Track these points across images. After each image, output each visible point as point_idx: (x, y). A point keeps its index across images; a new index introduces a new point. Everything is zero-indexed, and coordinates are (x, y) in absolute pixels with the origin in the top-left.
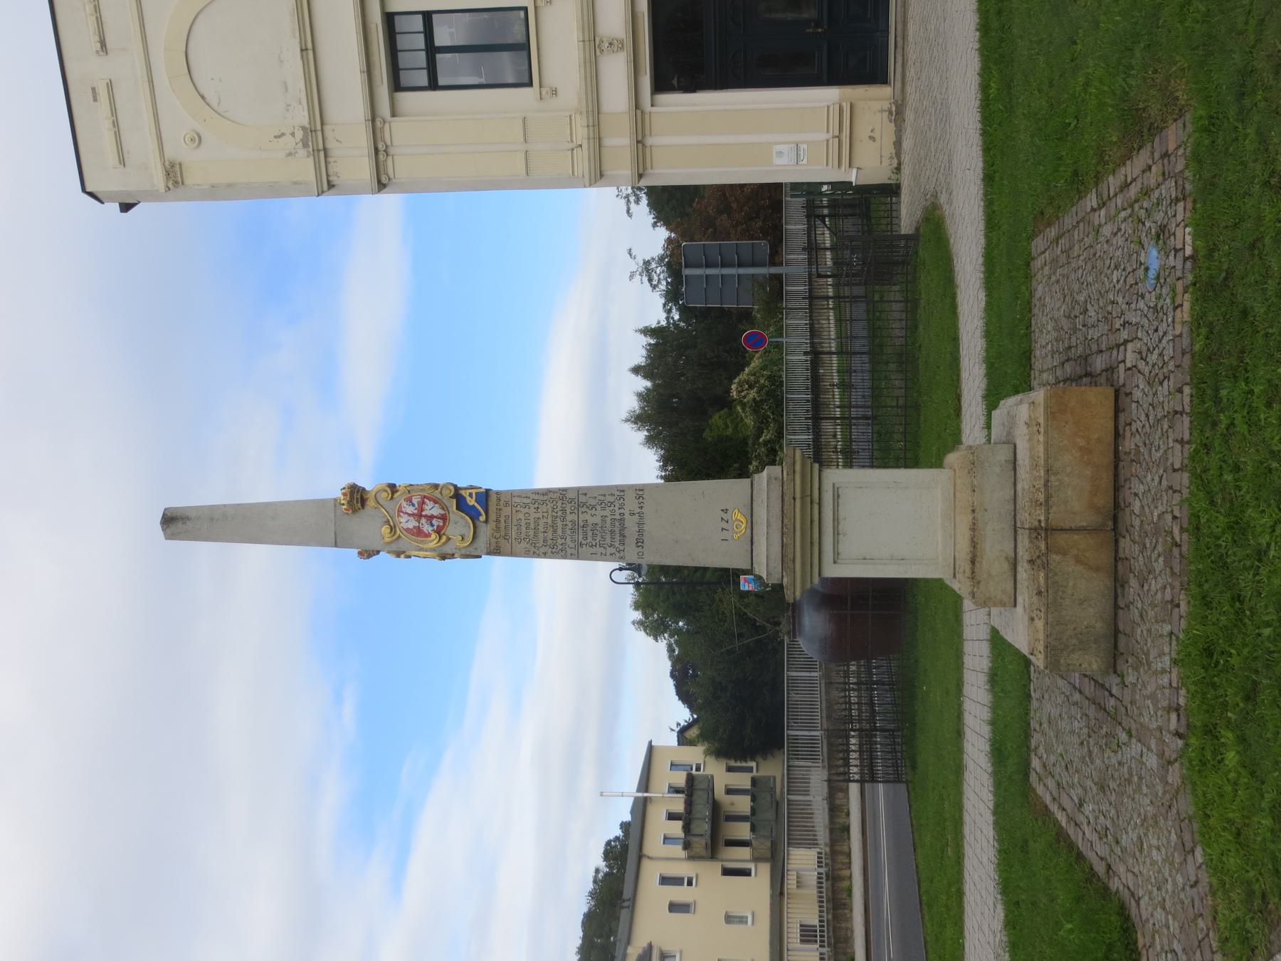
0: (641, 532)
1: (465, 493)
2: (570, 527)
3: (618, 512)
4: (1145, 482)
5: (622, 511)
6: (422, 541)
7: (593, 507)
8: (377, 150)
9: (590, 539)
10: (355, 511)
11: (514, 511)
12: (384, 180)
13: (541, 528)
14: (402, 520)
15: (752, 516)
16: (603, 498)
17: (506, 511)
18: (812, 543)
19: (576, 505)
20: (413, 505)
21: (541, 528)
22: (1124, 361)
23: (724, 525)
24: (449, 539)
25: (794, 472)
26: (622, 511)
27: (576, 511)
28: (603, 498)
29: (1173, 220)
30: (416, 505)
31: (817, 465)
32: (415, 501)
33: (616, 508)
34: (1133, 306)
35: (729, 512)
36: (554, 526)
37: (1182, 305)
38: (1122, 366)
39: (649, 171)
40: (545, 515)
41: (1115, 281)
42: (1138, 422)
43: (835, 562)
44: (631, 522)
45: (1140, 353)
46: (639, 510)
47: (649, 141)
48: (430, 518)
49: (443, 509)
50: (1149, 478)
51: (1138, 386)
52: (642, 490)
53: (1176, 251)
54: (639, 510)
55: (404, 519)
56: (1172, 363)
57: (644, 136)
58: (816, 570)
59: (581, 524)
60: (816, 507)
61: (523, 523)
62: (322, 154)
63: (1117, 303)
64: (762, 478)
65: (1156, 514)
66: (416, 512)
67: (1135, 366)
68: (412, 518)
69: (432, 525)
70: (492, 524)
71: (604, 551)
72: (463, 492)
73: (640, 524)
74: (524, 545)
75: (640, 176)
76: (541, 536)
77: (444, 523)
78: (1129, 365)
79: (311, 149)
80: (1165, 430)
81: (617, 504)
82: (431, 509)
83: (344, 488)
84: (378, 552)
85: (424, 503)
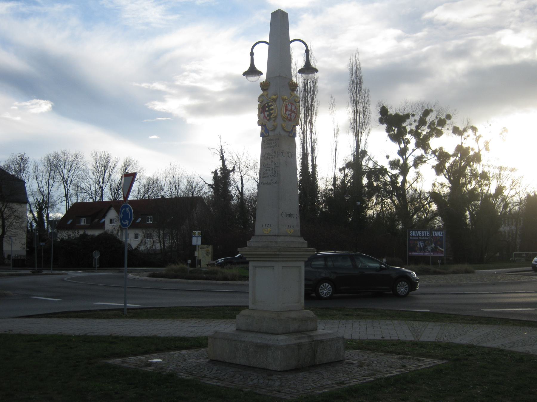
24: (284, 121)
31: (307, 260)
35: (270, 227)
48: (291, 115)
64: (302, 240)
69: (288, 115)
85: (295, 113)
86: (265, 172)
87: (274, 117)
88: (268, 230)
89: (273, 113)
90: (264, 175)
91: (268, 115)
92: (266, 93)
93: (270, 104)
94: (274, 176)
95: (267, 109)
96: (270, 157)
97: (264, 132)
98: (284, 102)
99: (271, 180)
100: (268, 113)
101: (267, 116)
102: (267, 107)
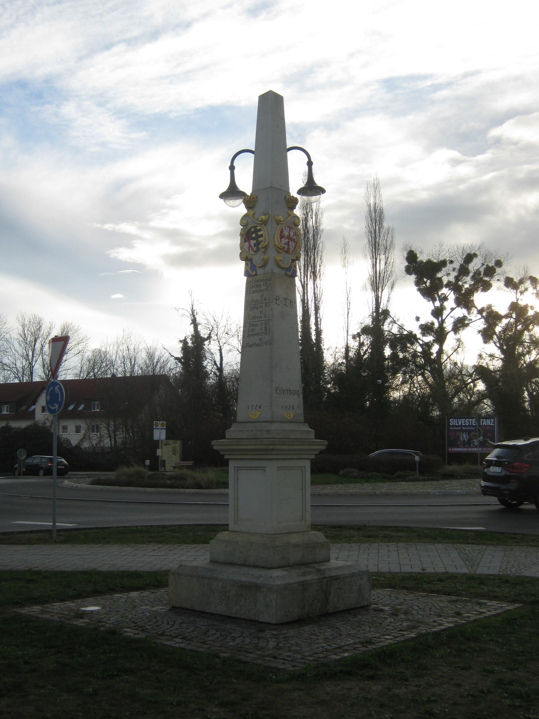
20: (293, 236)
24: (279, 253)
31: (313, 457)
48: (288, 244)
58: (233, 457)
64: (306, 428)
69: (285, 244)
85: (295, 242)
86: (252, 328)
87: (264, 247)
88: (256, 414)
89: (262, 241)
90: (250, 333)
91: (255, 245)
92: (251, 213)
93: (258, 228)
94: (265, 333)
95: (254, 235)
96: (258, 305)
97: (249, 270)
98: (278, 225)
99: (261, 340)
100: (255, 241)
101: (253, 246)
102: (253, 233)
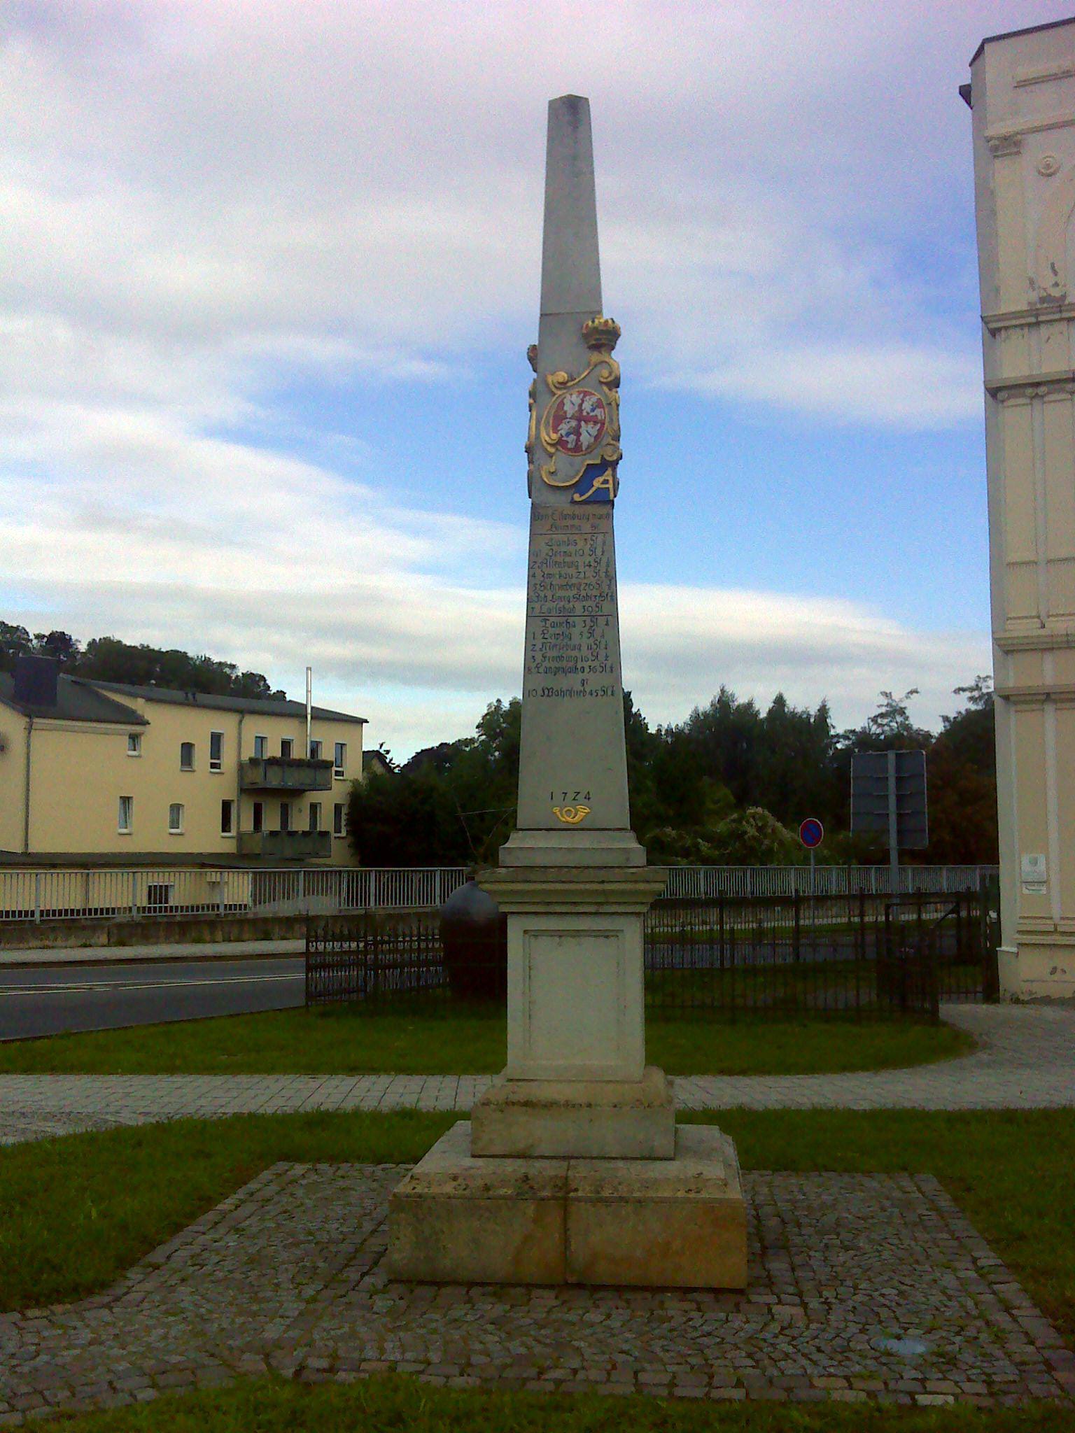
0: (561, 693)
1: (608, 475)
2: (567, 606)
3: (586, 665)
4: (624, 1329)
5: (587, 670)
6: (548, 422)
7: (591, 634)
8: (1037, 385)
9: (552, 631)
10: (586, 336)
11: (586, 536)
12: (1001, 395)
13: (565, 570)
14: (574, 396)
15: (583, 830)
16: (603, 646)
17: (587, 527)
18: (549, 903)
19: (593, 614)
20: (593, 410)
21: (565, 570)
22: (780, 1302)
23: (571, 795)
25: (636, 882)
26: (587, 670)
27: (586, 613)
28: (603, 646)
29: (963, 1377)
30: (592, 414)
32: (598, 412)
33: (589, 663)
34: (851, 1316)
36: (569, 586)
37: (851, 1387)
38: (774, 1299)
39: (1013, 708)
40: (582, 575)
41: (884, 1291)
42: (701, 1321)
43: (526, 932)
44: (573, 681)
45: (790, 1326)
46: (588, 690)
47: (1049, 708)
49: (589, 447)
50: (628, 1335)
51: (748, 1322)
52: (612, 695)
53: (923, 1381)
54: (588, 690)
55: (576, 399)
56: (776, 1373)
57: (1055, 701)
59: (570, 620)
60: (592, 909)
61: (572, 548)
62: (1033, 320)
63: (855, 1294)
64: (630, 843)
65: (582, 1344)
66: (585, 414)
67: (773, 1317)
68: (577, 408)
69: (568, 434)
70: (569, 509)
71: (537, 648)
72: (609, 472)
73: (570, 692)
74: (545, 549)
75: (1006, 698)
76: (555, 571)
77: (570, 450)
78: (775, 1309)
79: (1039, 306)
80: (689, 1359)
81: (596, 663)
82: (588, 432)
83: (613, 322)
84: (535, 371)
85: (595, 423)
